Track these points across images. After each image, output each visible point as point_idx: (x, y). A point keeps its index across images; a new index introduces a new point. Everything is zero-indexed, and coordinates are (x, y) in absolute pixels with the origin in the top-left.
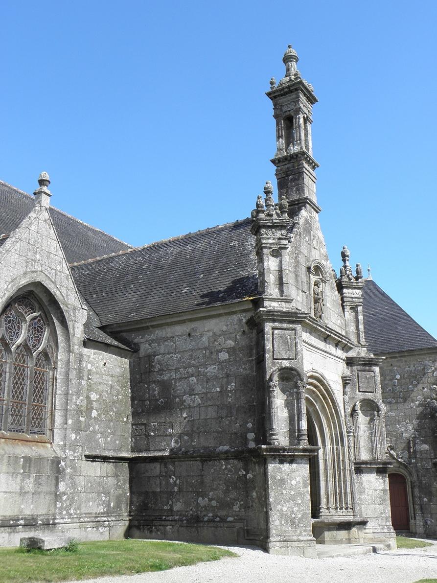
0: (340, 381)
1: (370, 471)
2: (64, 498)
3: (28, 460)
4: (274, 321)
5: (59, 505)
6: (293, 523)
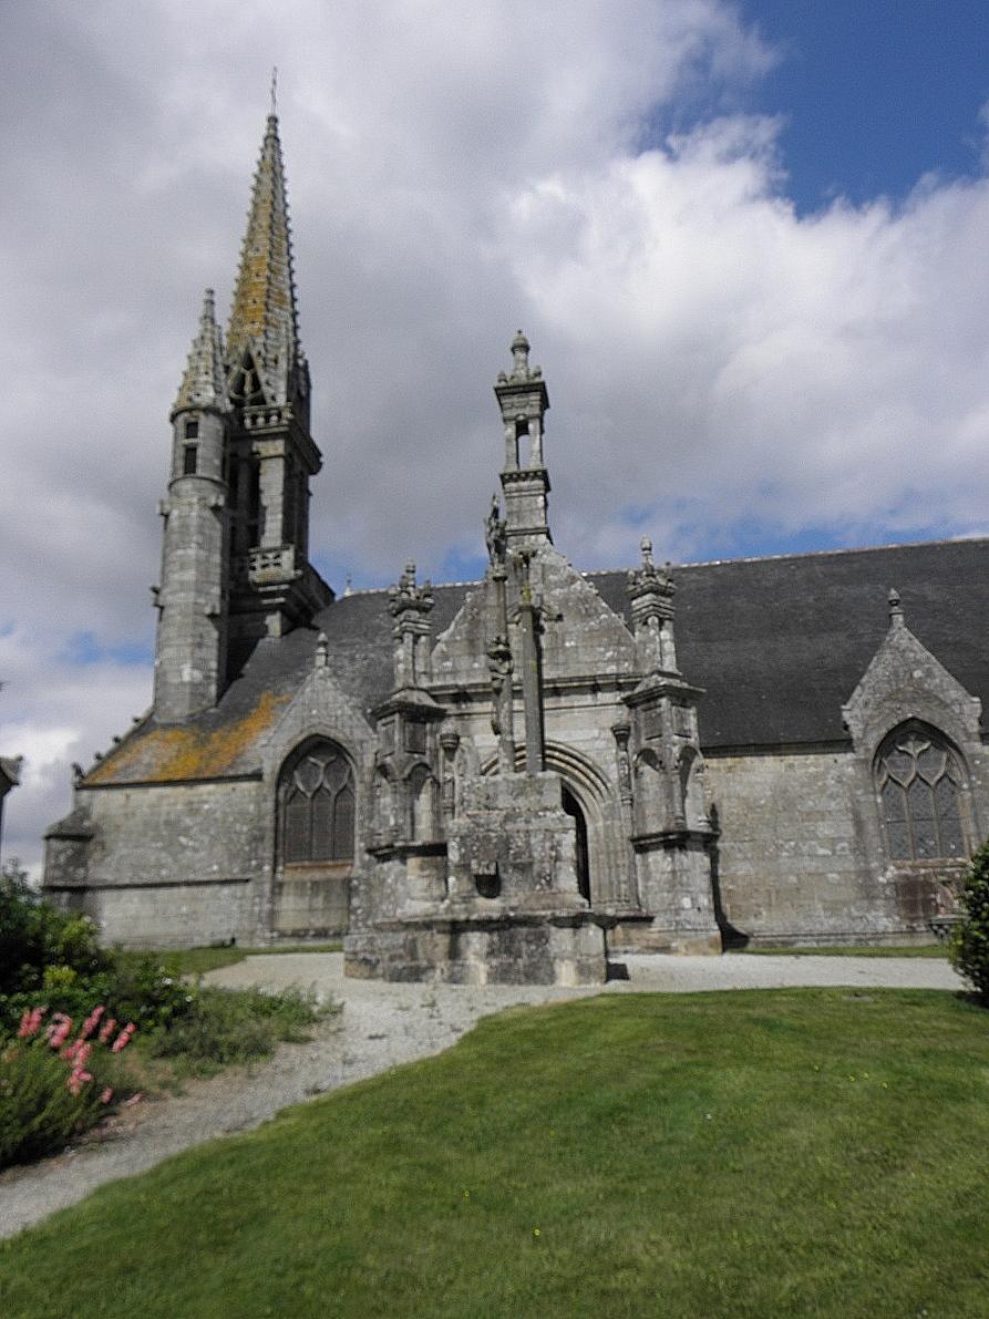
0: (610, 734)
1: (655, 847)
2: (359, 911)
3: (315, 884)
4: (380, 718)
5: (353, 917)
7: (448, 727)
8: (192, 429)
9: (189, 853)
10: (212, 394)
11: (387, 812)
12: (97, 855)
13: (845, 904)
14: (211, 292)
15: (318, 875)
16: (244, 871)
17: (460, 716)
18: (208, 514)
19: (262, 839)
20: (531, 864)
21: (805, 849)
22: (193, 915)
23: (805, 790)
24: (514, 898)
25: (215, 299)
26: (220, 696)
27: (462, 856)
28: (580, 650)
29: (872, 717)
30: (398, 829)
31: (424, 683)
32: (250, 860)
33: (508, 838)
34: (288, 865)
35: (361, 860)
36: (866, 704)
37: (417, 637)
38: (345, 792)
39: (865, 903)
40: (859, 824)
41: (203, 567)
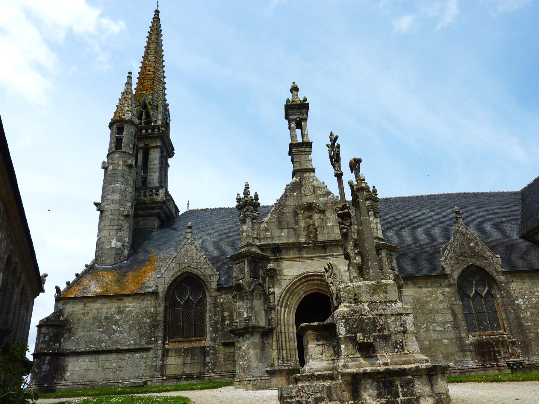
2: (210, 364)
3: (186, 350)
5: (207, 368)
6: (244, 370)
7: (271, 265)
8: (120, 130)
9: (117, 334)
10: (130, 115)
11: (241, 310)
12: (66, 336)
13: (452, 354)
14: (130, 73)
15: (187, 345)
16: (147, 343)
17: (276, 260)
18: (125, 168)
19: (157, 326)
20: (390, 336)
21: (431, 327)
22: (119, 368)
23: (428, 299)
24: (385, 360)
25: (132, 76)
26: (129, 256)
27: (348, 332)
28: (334, 227)
29: (455, 264)
30: (249, 319)
31: (257, 243)
32: (151, 338)
33: (374, 321)
34: (171, 340)
35: (211, 337)
36: (451, 258)
37: (253, 219)
38: (202, 302)
39: (461, 354)
40: (454, 314)
41: (123, 193)
